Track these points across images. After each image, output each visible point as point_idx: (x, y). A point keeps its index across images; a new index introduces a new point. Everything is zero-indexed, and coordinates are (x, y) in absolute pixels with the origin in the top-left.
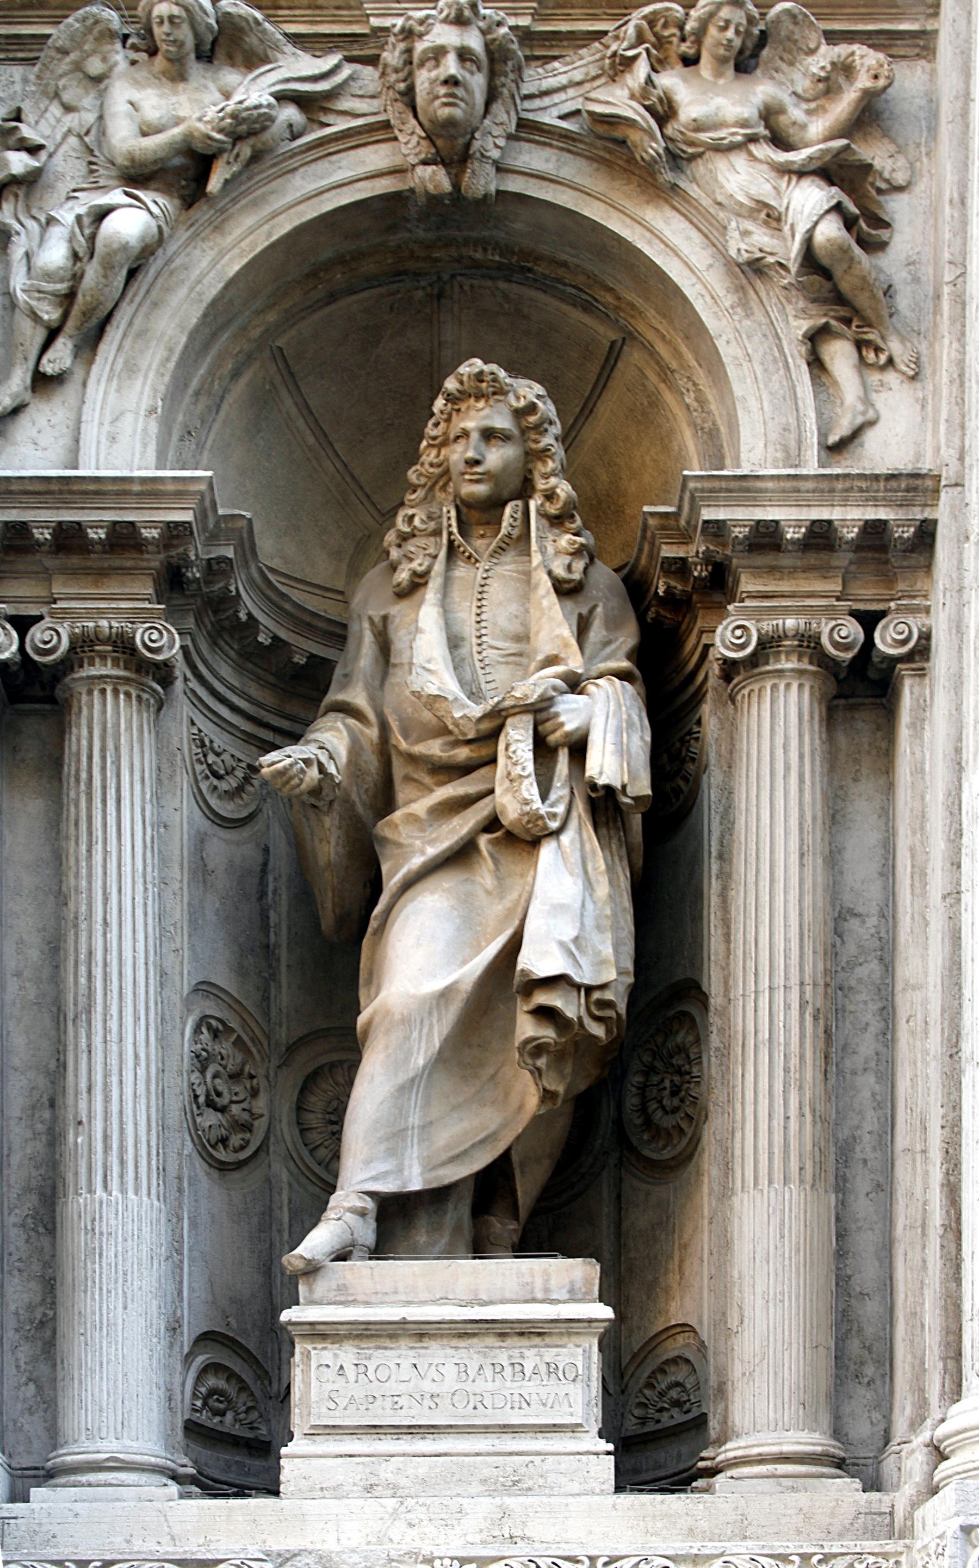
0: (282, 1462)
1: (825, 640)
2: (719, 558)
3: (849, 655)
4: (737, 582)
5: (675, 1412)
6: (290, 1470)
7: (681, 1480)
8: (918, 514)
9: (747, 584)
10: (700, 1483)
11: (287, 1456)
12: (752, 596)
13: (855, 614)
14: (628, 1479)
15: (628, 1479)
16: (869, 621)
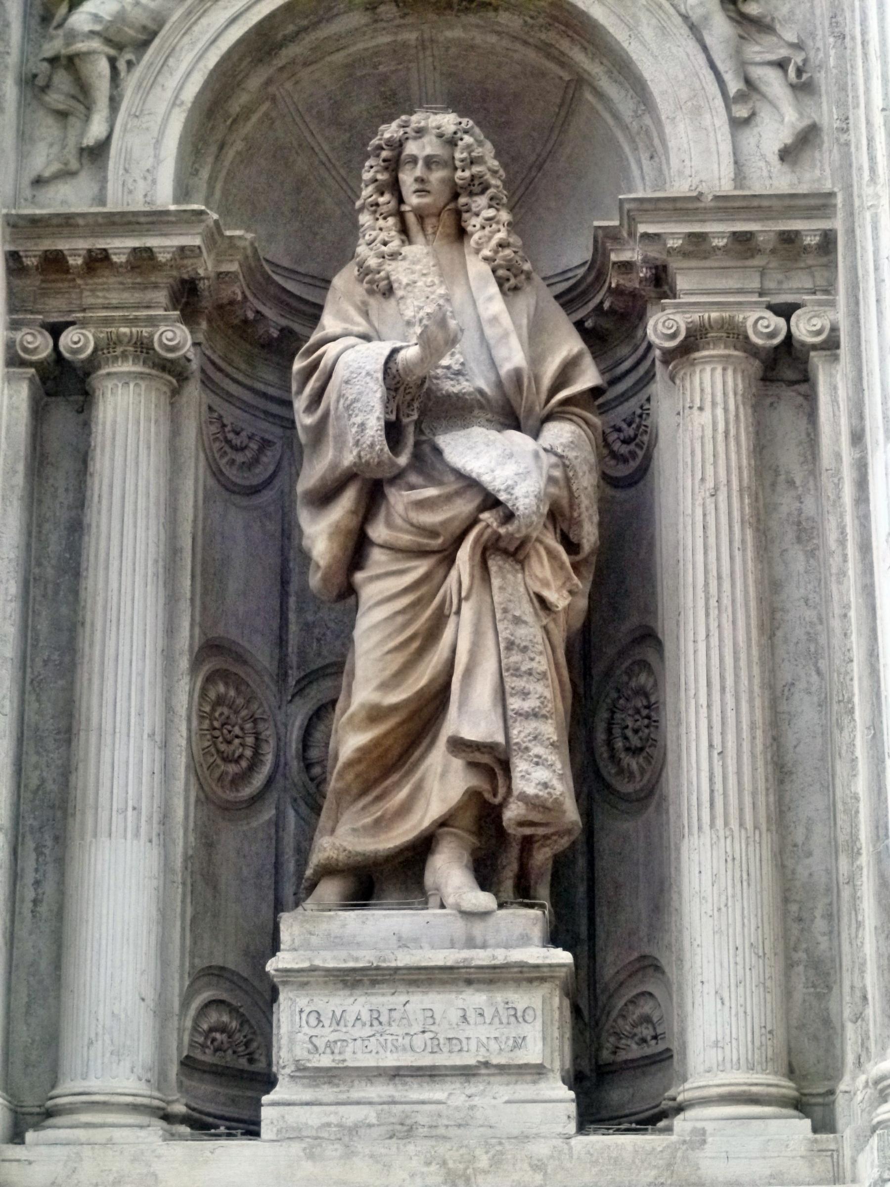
1: (750, 332)
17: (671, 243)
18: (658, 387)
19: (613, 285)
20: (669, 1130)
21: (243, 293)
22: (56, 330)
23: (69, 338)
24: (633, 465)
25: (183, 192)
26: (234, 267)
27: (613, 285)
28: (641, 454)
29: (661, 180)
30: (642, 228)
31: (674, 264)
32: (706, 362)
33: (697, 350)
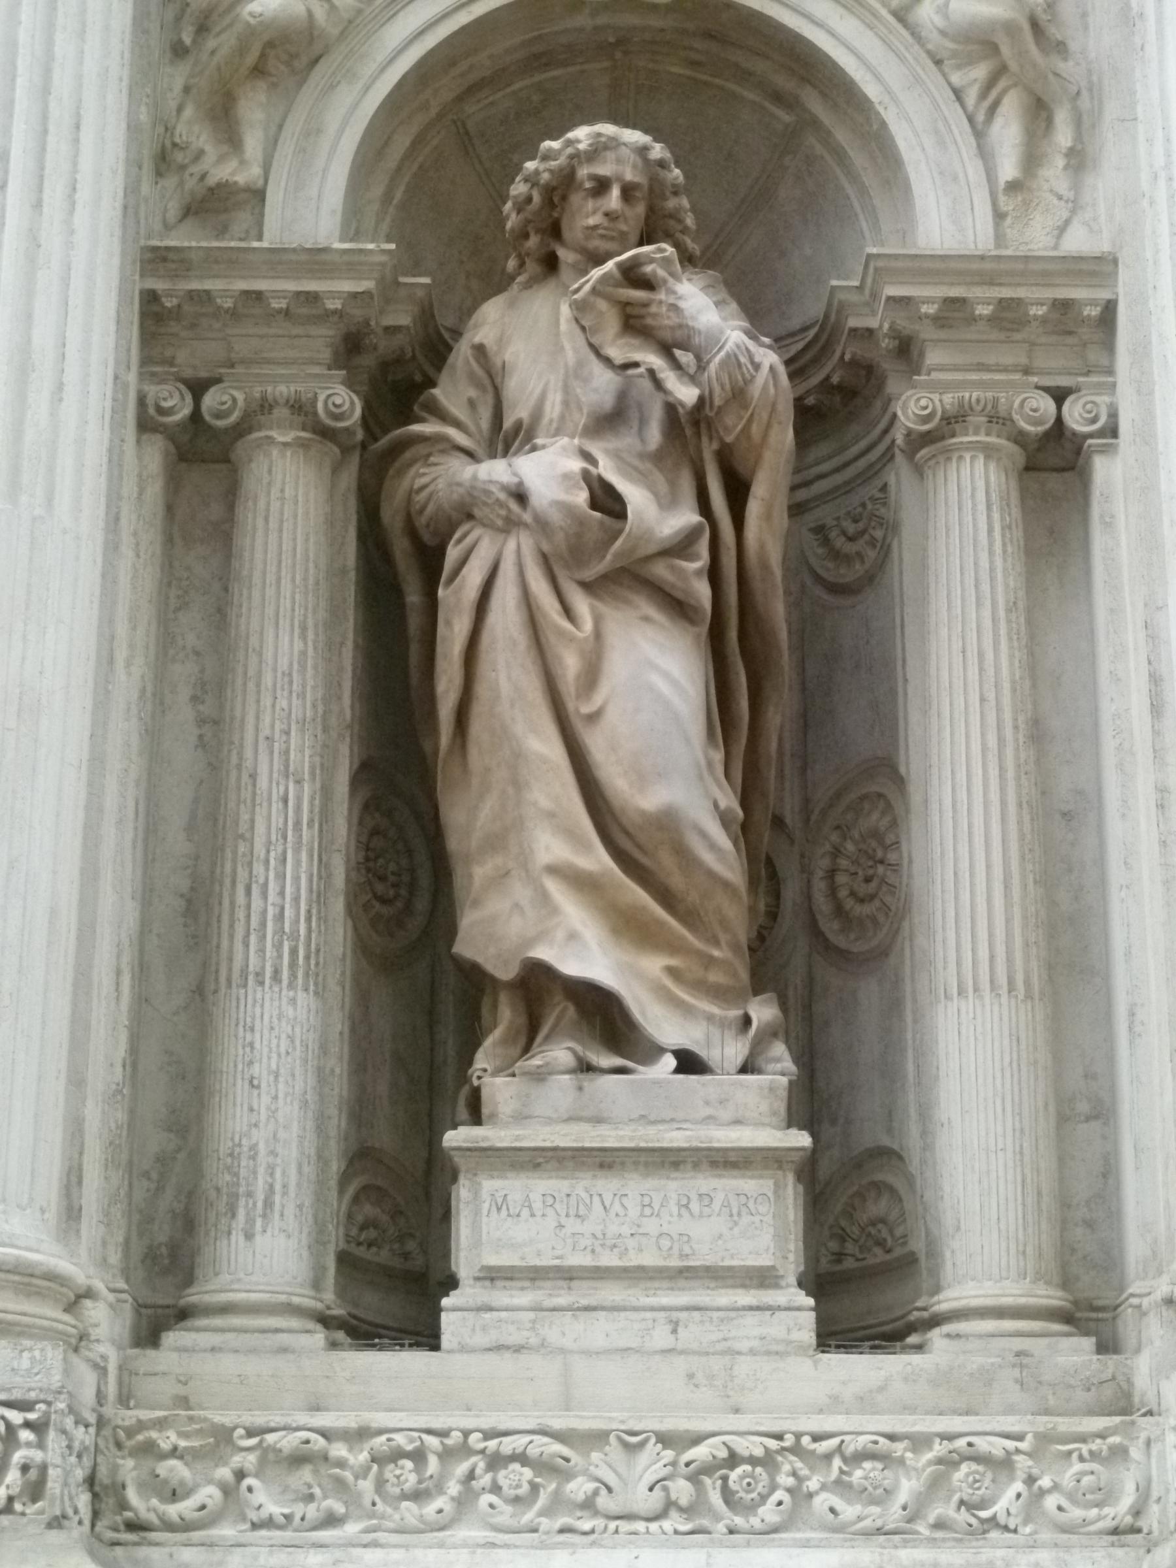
0: (443, 1315)
2: (906, 332)
3: (1040, 429)
4: (922, 354)
5: (878, 1251)
6: (450, 1323)
7: (892, 1335)
8: (1104, 295)
9: (933, 357)
10: (912, 1339)
11: (448, 1310)
12: (942, 368)
13: (1047, 390)
14: (833, 1336)
15: (833, 1336)
16: (1060, 396)
17: (924, 309)
18: (900, 476)
19: (847, 357)
20: (919, 1348)
21: (413, 351)
22: (197, 388)
23: (210, 400)
24: (859, 569)
25: (352, 225)
26: (405, 320)
27: (847, 357)
28: (871, 554)
29: (905, 235)
30: (892, 291)
31: (927, 332)
32: (967, 449)
33: (953, 436)
